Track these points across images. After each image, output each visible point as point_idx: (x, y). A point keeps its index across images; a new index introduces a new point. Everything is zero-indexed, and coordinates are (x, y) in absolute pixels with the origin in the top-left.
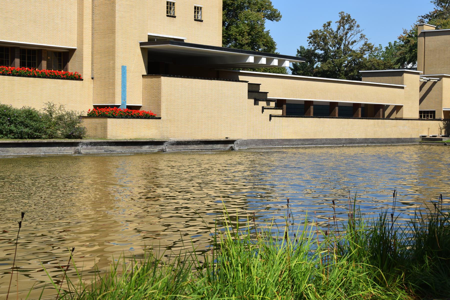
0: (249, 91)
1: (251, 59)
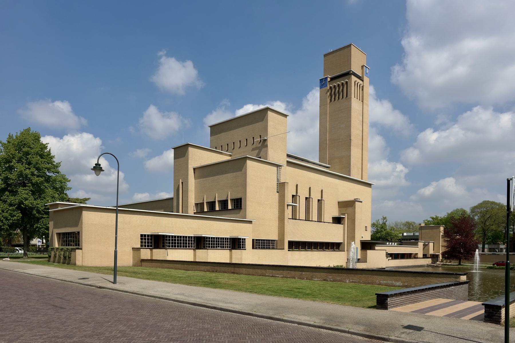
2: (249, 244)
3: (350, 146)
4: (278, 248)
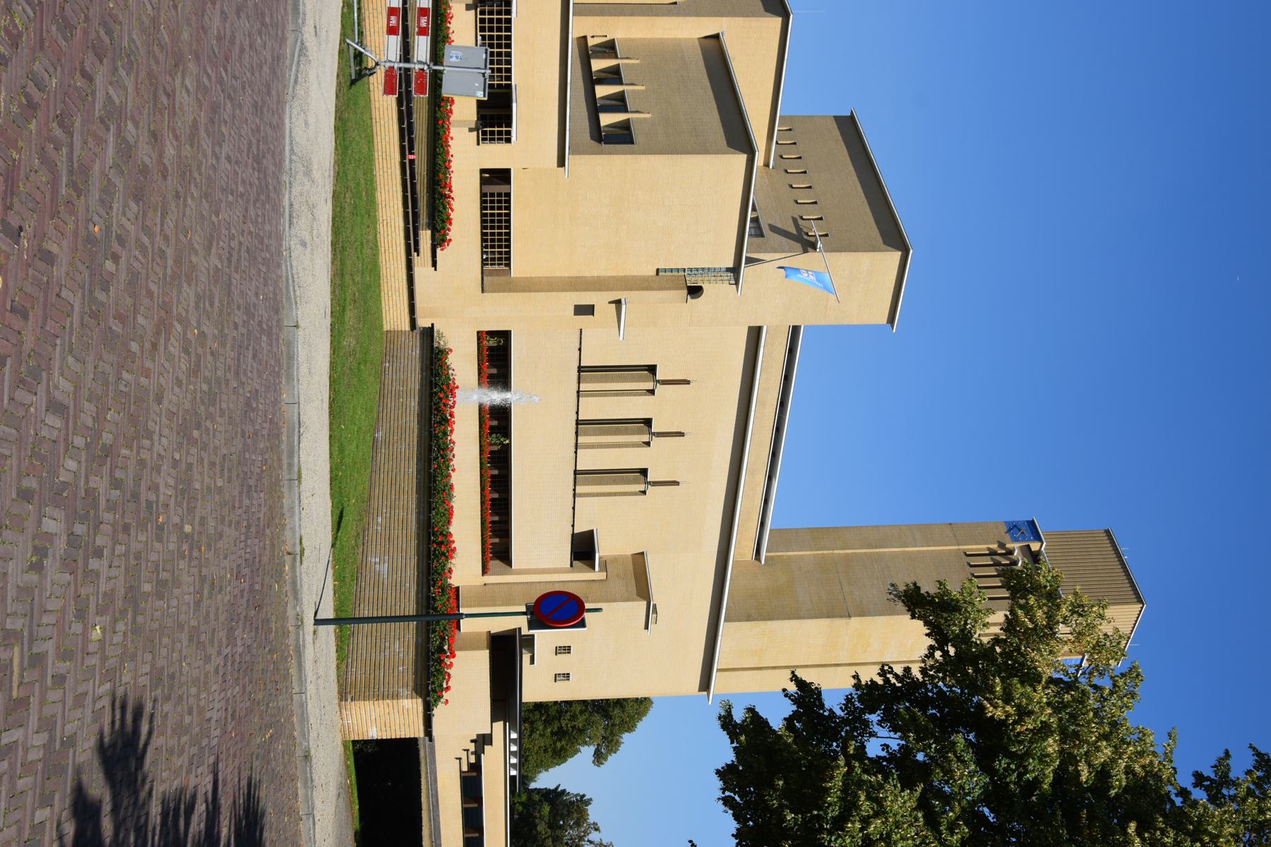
0: (484, 735)
1: (514, 736)
2: (495, 155)
3: (828, 617)
4: (485, 278)
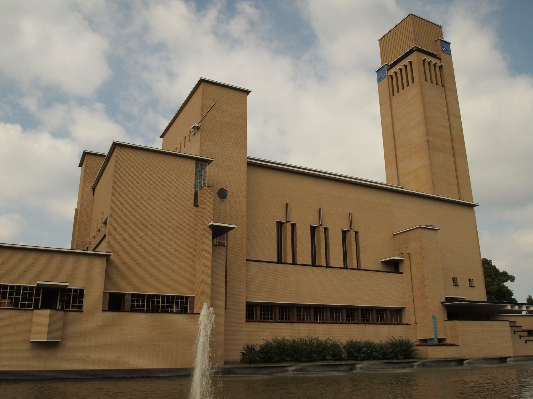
1: (509, 307)
4: (195, 312)
